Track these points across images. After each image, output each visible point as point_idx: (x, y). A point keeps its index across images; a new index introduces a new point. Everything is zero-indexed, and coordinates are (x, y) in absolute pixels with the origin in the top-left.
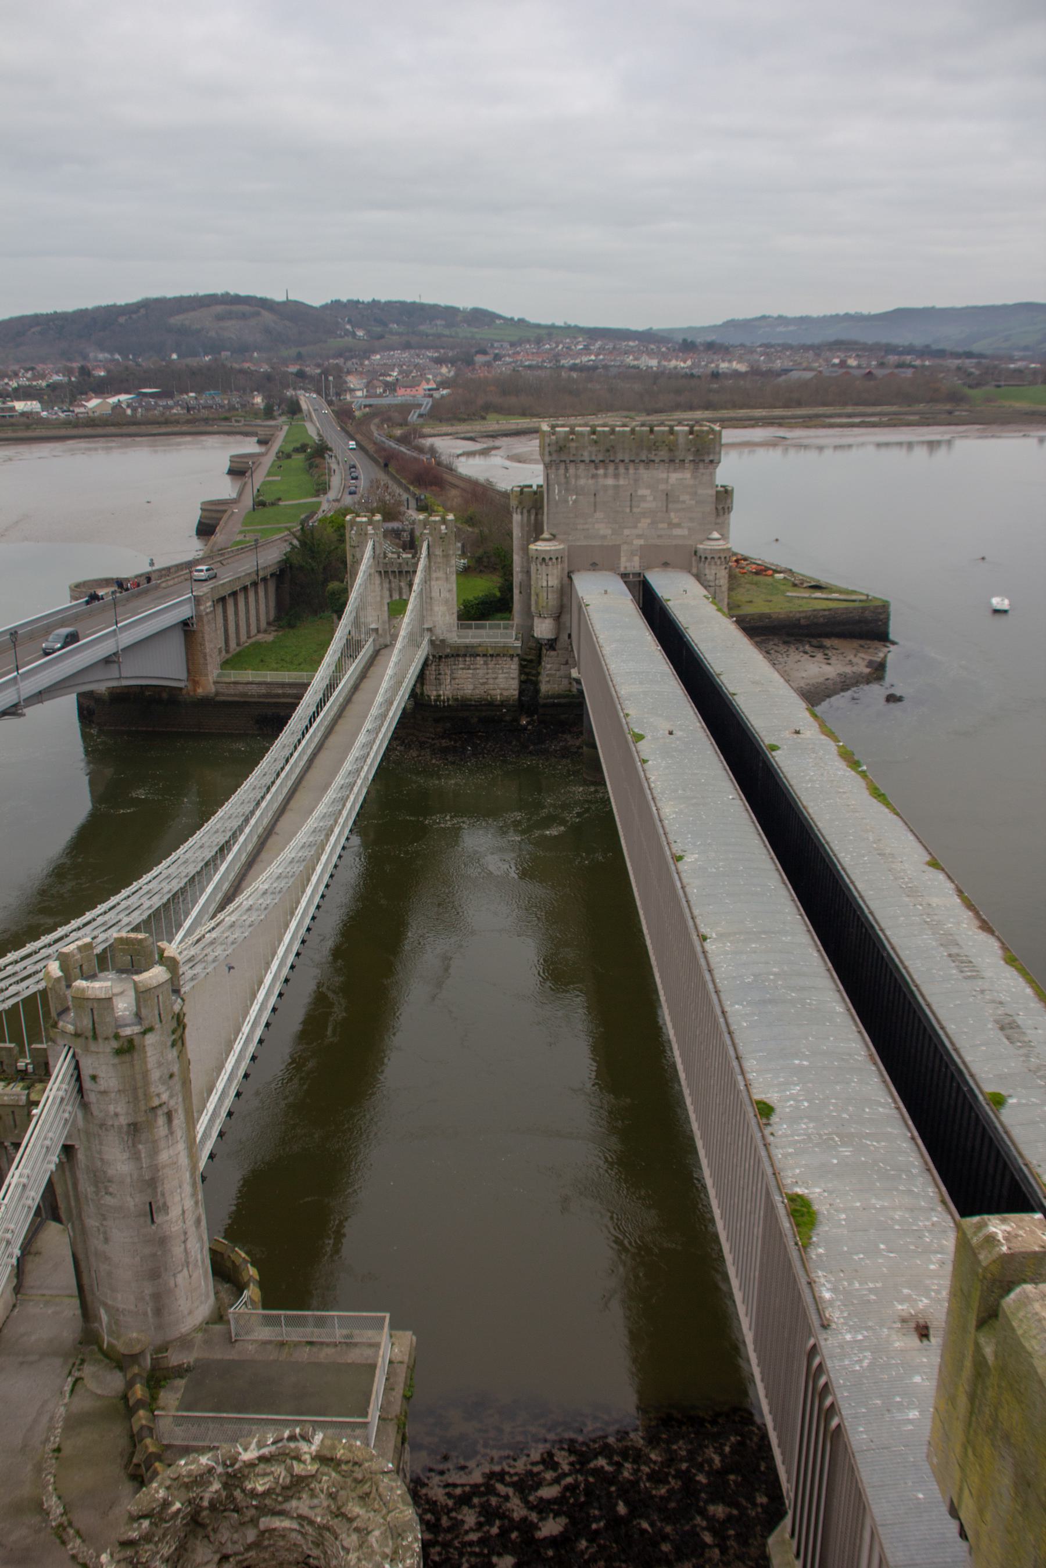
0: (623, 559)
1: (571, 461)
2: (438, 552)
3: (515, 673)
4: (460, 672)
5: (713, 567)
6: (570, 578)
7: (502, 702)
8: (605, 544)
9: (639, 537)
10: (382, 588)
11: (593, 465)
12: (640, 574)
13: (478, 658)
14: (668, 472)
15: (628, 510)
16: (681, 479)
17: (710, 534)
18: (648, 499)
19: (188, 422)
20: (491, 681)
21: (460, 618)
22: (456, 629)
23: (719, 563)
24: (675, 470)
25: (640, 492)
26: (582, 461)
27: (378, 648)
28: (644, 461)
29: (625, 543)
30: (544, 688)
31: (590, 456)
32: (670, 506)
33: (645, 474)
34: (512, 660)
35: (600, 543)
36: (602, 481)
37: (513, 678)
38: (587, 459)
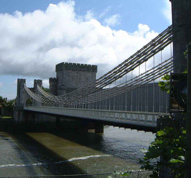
32: (87, 81)
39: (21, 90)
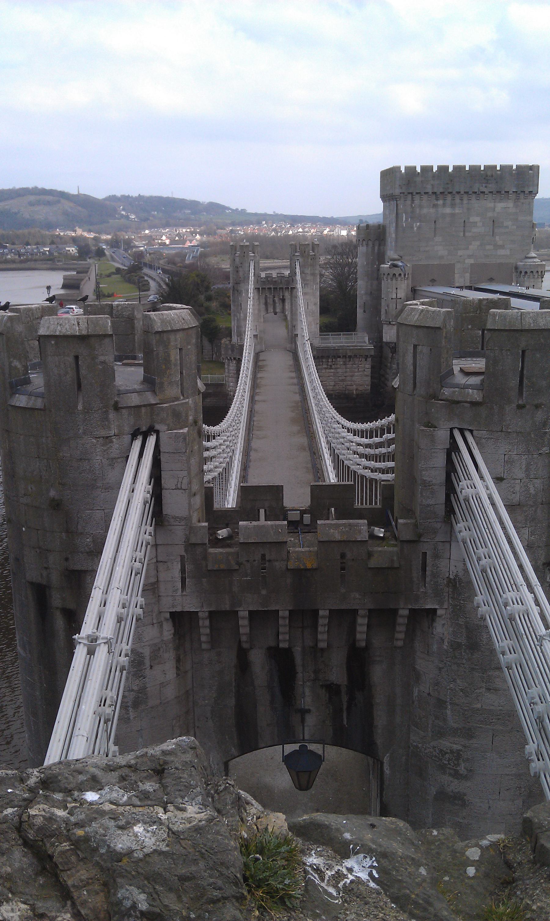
0: (456, 276)
1: (417, 193)
2: (308, 271)
3: (368, 372)
4: (324, 371)
5: (532, 280)
7: (357, 395)
8: (443, 263)
9: (470, 257)
10: (260, 302)
11: (434, 197)
13: (338, 359)
14: (495, 202)
15: (462, 234)
17: (528, 254)
19: (21, 262)
20: (348, 378)
21: (321, 330)
22: (318, 336)
23: (536, 276)
24: (501, 200)
25: (472, 219)
26: (426, 193)
27: (257, 351)
29: (459, 262)
31: (433, 188)
32: (496, 231)
33: (476, 204)
35: (438, 263)
36: (441, 210)
37: (367, 376)
38: (430, 191)
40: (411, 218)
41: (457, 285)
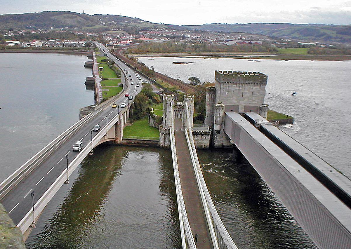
6: (225, 114)
9: (244, 103)
12: (244, 114)
16: (256, 88)
18: (247, 94)
20: (202, 142)
24: (255, 86)
28: (247, 83)
30: (216, 143)
32: (253, 95)
33: (247, 87)
34: (208, 136)
37: (208, 141)
39: (167, 109)
40: (226, 90)
41: (240, 112)
